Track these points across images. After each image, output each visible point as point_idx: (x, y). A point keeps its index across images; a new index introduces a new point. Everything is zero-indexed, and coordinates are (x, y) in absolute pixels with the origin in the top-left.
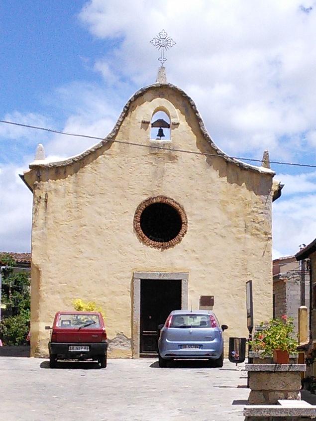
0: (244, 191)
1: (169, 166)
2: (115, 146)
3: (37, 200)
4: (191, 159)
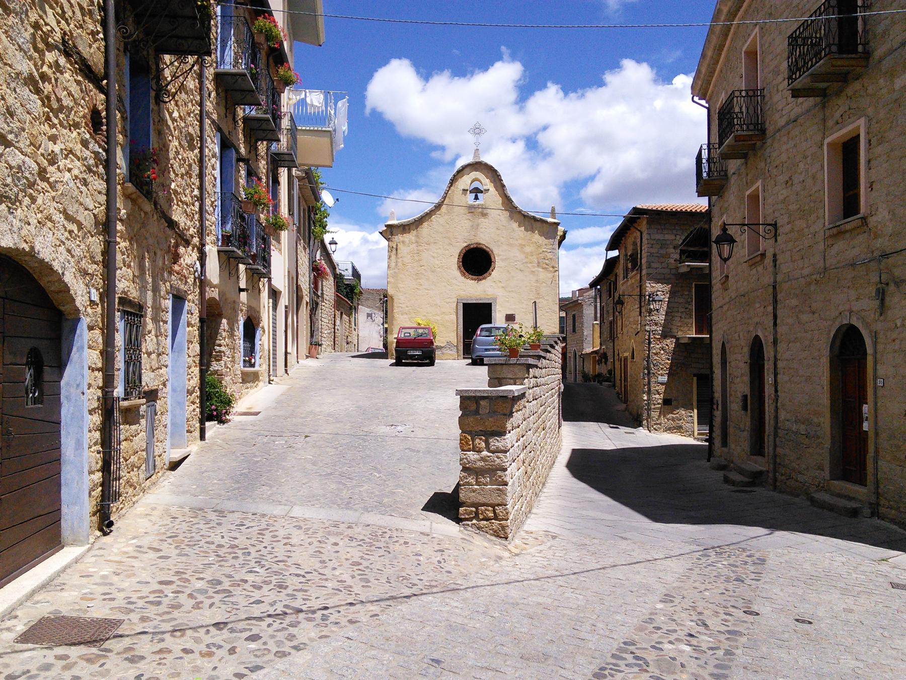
0: (537, 237)
1: (483, 221)
2: (444, 207)
3: (391, 248)
4: (498, 215)
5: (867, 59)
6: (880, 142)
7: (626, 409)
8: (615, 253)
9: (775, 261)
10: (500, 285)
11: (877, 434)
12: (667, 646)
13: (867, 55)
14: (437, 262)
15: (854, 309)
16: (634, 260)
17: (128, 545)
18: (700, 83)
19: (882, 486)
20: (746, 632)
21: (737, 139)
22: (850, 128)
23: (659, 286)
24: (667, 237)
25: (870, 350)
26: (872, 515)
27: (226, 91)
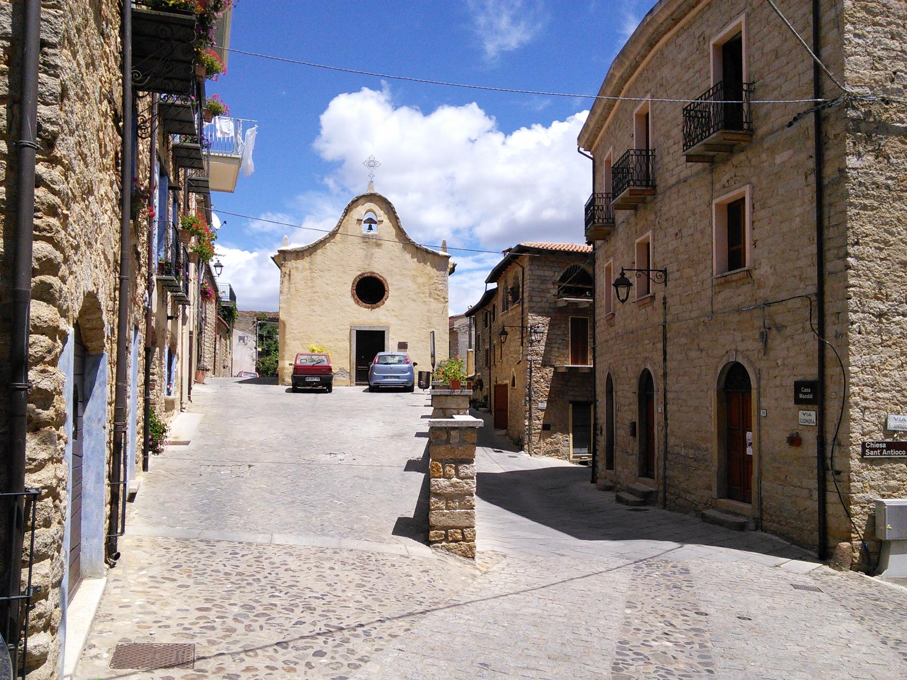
0: (429, 269)
1: (376, 250)
2: (338, 236)
3: (283, 275)
4: (392, 246)
5: (751, 136)
6: (763, 207)
7: (506, 434)
8: (494, 286)
9: (665, 303)
10: (393, 313)
11: (760, 457)
12: (653, 643)
13: (751, 132)
14: (331, 289)
15: (739, 349)
16: (515, 294)
17: (140, 576)
18: (587, 136)
19: (764, 503)
20: (706, 629)
21: (632, 193)
22: (737, 192)
23: (539, 319)
24: (547, 273)
25: (754, 384)
26: (756, 529)
27: (165, 120)
